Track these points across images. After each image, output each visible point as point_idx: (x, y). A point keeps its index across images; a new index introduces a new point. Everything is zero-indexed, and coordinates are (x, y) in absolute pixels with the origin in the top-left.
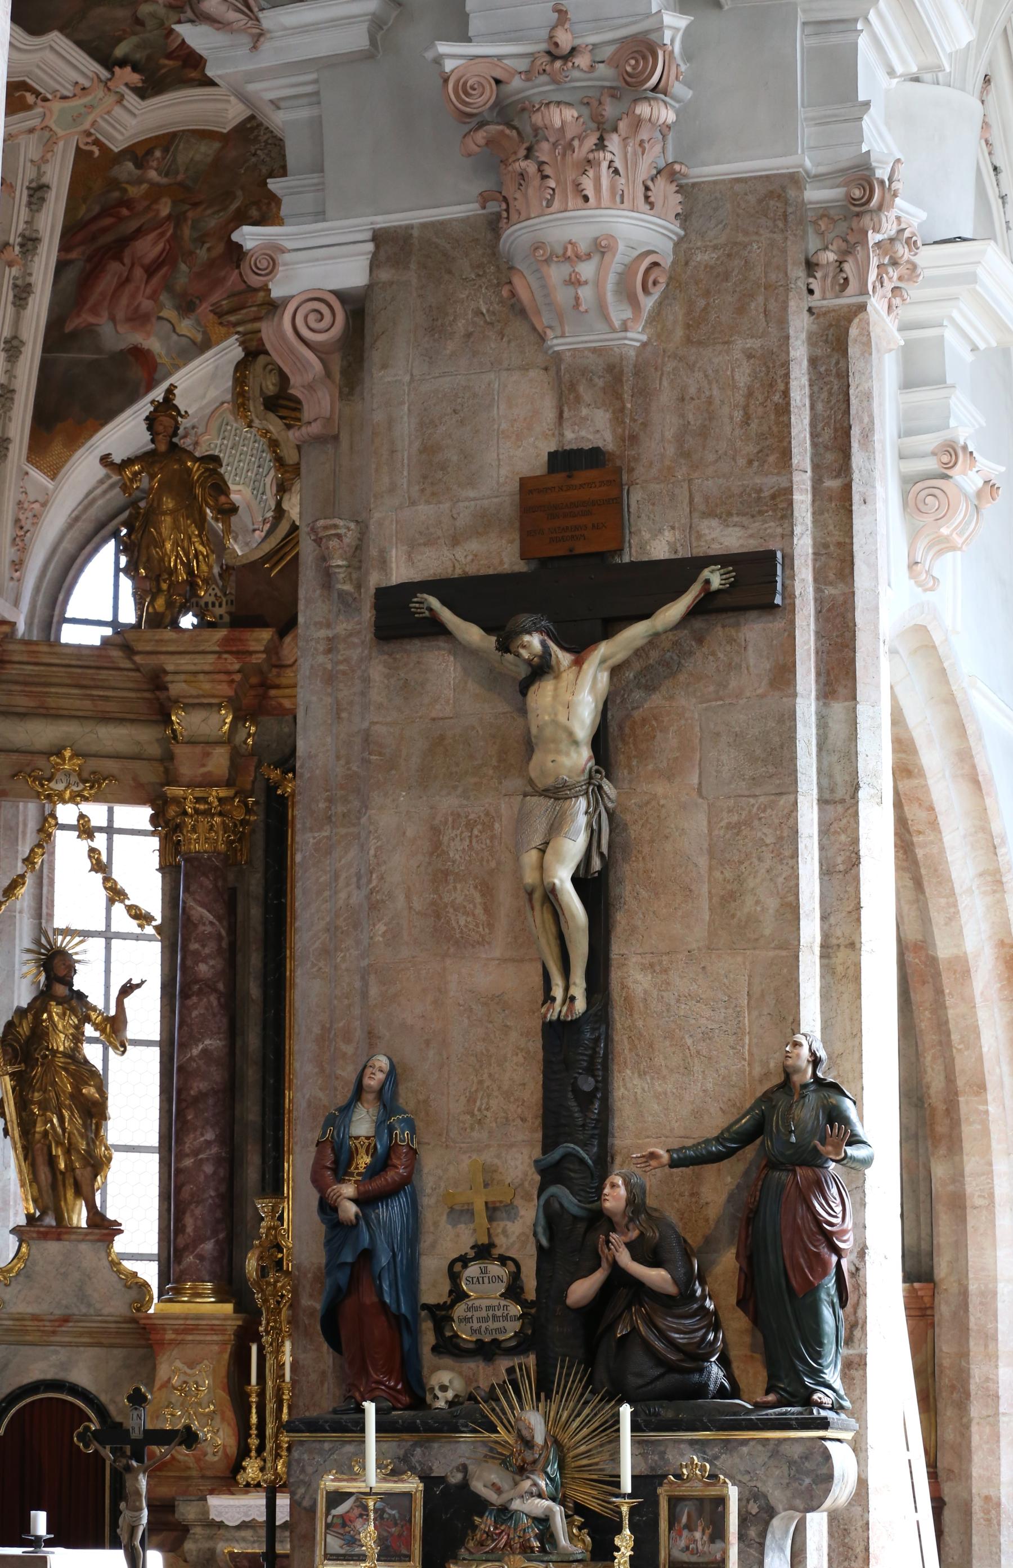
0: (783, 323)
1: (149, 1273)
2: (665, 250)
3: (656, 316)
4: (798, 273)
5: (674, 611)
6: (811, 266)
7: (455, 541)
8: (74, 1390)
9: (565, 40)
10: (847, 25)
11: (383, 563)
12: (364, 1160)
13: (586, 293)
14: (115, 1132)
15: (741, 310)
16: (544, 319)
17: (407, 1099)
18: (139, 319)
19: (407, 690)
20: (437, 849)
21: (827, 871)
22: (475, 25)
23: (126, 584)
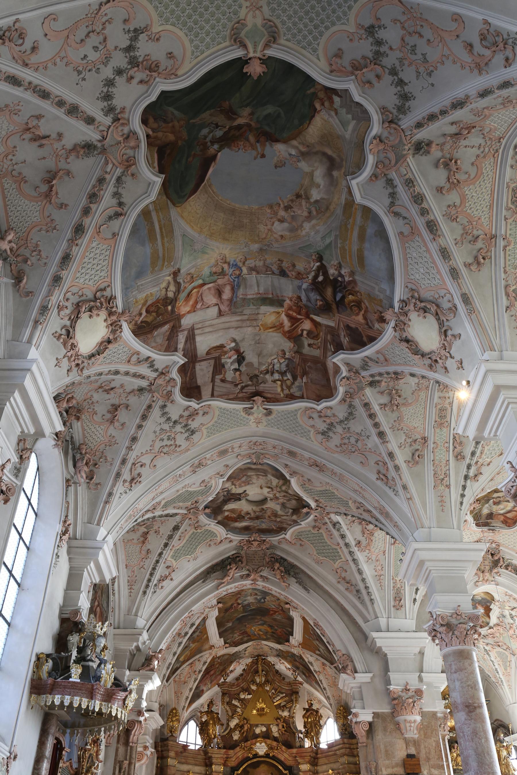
9: (408, 688)
13: (412, 728)
15: (432, 733)
16: (404, 731)
18: (205, 684)
23: (199, 737)
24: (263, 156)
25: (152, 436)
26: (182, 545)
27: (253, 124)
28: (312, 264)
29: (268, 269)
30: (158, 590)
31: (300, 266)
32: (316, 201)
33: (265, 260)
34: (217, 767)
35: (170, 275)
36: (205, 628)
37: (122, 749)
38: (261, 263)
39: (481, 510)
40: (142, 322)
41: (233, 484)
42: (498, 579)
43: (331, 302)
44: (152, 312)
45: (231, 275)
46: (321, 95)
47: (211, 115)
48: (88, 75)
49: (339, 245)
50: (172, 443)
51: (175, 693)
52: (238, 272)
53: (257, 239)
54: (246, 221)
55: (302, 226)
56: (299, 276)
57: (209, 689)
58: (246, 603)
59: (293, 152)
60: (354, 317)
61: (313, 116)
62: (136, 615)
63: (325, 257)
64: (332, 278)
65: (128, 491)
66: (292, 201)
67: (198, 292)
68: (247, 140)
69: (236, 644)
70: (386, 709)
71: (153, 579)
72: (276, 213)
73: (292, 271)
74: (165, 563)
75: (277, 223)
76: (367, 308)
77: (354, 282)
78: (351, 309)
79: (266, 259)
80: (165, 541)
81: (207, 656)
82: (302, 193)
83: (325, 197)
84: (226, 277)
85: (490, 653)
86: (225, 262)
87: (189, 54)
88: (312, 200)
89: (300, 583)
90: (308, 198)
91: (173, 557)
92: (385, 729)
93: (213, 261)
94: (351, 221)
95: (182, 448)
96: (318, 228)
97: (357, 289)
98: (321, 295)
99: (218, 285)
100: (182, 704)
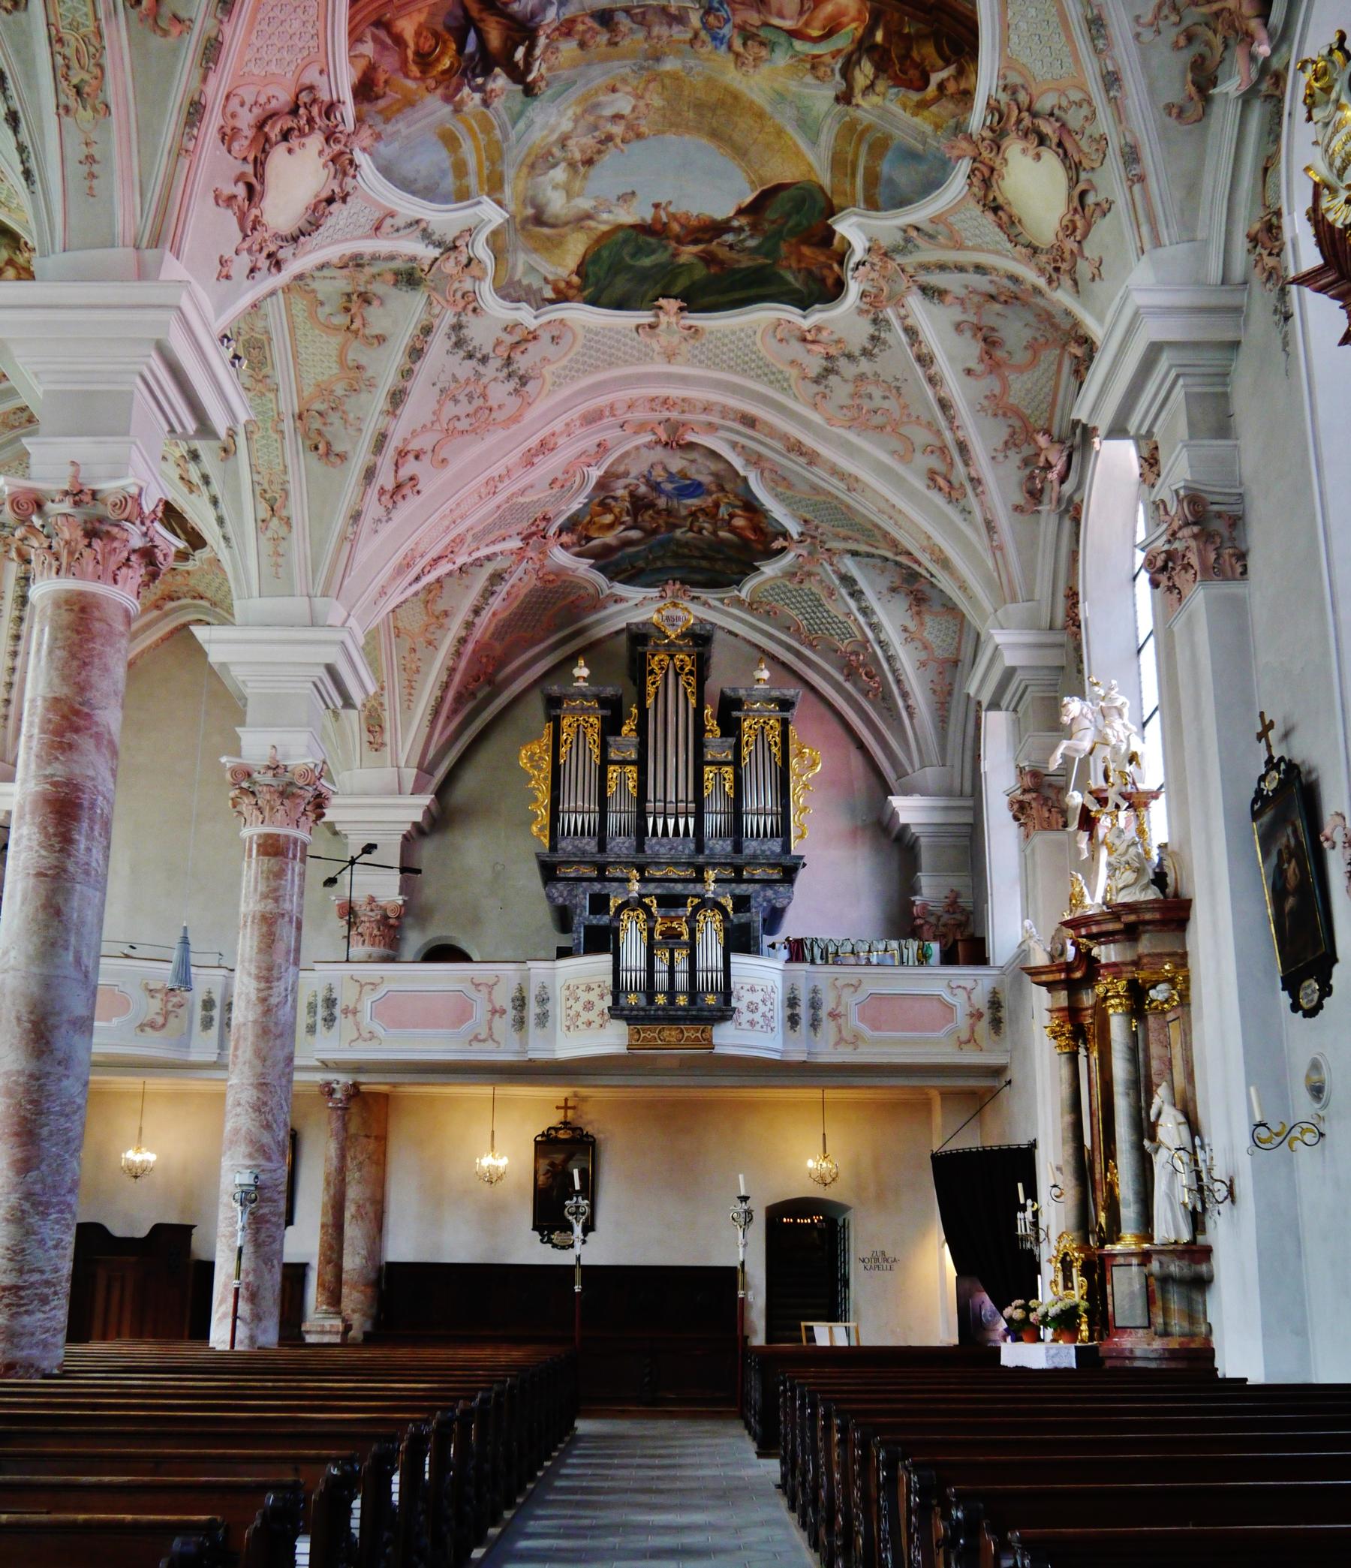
24: (657, 206)
27: (673, 244)
28: (543, 70)
29: (640, 18)
31: (568, 48)
32: (554, 166)
33: (649, 37)
35: (858, 106)
38: (656, 30)
40: (948, 63)
43: (484, 15)
44: (917, 66)
45: (727, 21)
46: (572, 292)
47: (738, 261)
48: (890, 379)
49: (497, 132)
52: (711, 19)
53: (667, 81)
54: (691, 115)
55: (576, 121)
56: (567, 29)
59: (605, 216)
60: (422, 17)
61: (579, 266)
63: (520, 97)
64: (497, 70)
66: (599, 152)
67: (807, 24)
68: (682, 226)
72: (630, 127)
73: (584, 32)
75: (626, 110)
76: (407, 75)
77: (448, 99)
78: (436, 35)
79: (646, 39)
82: (582, 169)
83: (542, 178)
84: (738, 20)
86: (737, 55)
87: (759, 335)
88: (563, 165)
90: (572, 165)
93: (765, 69)
94: (486, 172)
96: (545, 132)
97: (440, 91)
98: (511, 17)
99: (759, 12)
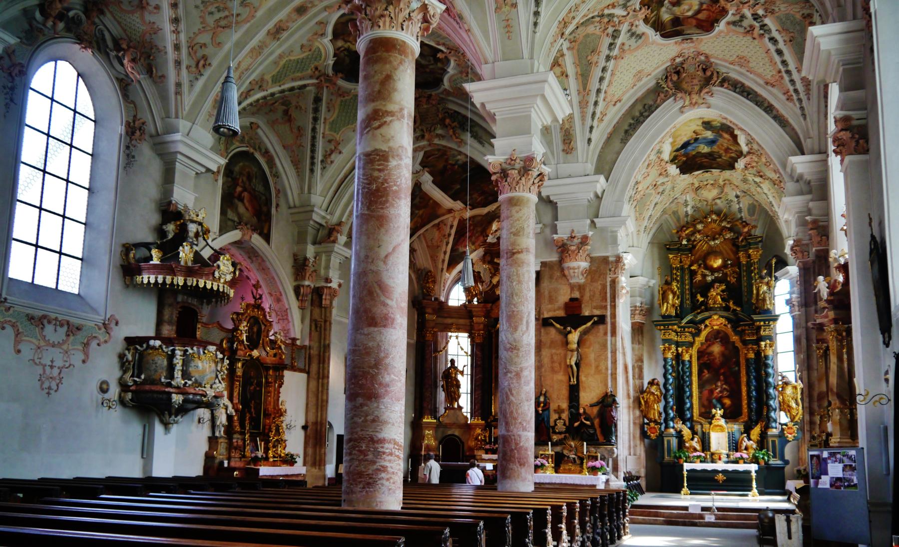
0: (606, 279)
1: (469, 416)
2: (588, 267)
3: (586, 278)
4: (608, 272)
5: (589, 324)
6: (610, 270)
7: (555, 311)
8: (455, 436)
9: (573, 235)
10: (616, 232)
11: (543, 314)
12: (542, 405)
14: (461, 390)
15: (599, 277)
16: (568, 278)
17: (548, 395)
19: (547, 334)
20: (552, 358)
21: (612, 363)
22: (558, 232)
25: (195, 13)
26: (335, 116)
30: (327, 165)
34: (478, 319)
36: (426, 194)
37: (317, 311)
39: (658, 16)
41: (346, 41)
42: (711, 100)
50: (226, 13)
51: (431, 257)
57: (475, 250)
58: (460, 162)
62: (309, 192)
65: (198, 77)
69: (485, 205)
70: (554, 258)
71: (316, 156)
74: (323, 137)
80: (311, 116)
81: (451, 219)
85: (761, 185)
89: (475, 136)
91: (331, 129)
92: (551, 277)
95: (244, 16)
100: (440, 266)
